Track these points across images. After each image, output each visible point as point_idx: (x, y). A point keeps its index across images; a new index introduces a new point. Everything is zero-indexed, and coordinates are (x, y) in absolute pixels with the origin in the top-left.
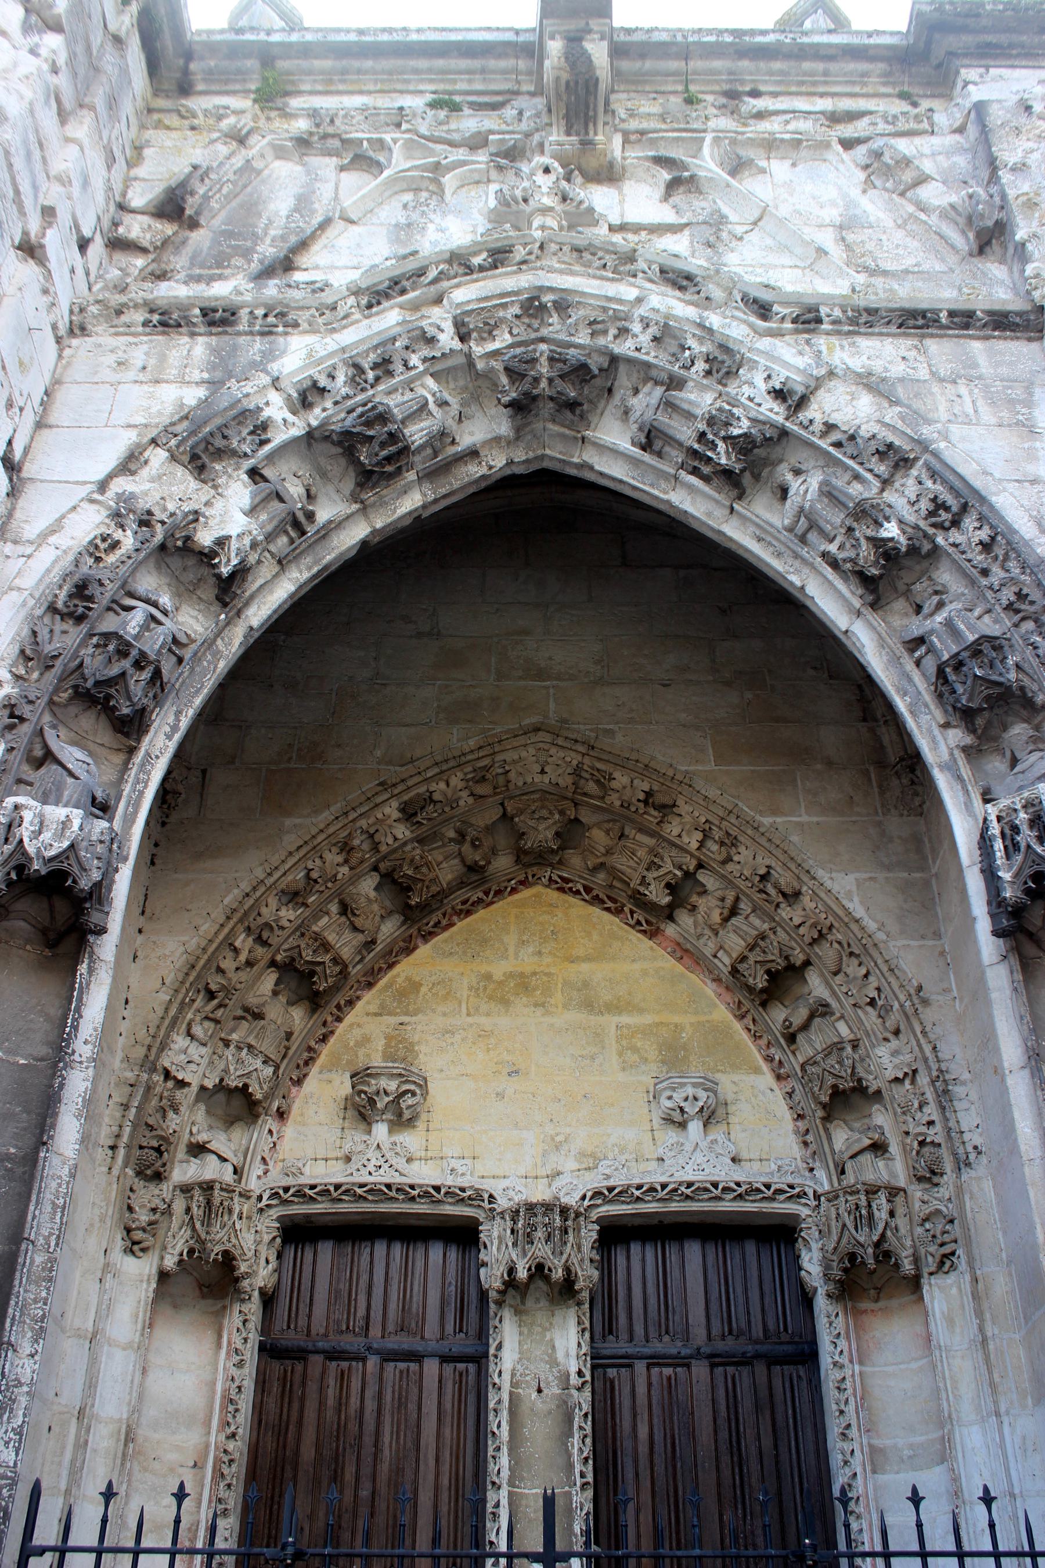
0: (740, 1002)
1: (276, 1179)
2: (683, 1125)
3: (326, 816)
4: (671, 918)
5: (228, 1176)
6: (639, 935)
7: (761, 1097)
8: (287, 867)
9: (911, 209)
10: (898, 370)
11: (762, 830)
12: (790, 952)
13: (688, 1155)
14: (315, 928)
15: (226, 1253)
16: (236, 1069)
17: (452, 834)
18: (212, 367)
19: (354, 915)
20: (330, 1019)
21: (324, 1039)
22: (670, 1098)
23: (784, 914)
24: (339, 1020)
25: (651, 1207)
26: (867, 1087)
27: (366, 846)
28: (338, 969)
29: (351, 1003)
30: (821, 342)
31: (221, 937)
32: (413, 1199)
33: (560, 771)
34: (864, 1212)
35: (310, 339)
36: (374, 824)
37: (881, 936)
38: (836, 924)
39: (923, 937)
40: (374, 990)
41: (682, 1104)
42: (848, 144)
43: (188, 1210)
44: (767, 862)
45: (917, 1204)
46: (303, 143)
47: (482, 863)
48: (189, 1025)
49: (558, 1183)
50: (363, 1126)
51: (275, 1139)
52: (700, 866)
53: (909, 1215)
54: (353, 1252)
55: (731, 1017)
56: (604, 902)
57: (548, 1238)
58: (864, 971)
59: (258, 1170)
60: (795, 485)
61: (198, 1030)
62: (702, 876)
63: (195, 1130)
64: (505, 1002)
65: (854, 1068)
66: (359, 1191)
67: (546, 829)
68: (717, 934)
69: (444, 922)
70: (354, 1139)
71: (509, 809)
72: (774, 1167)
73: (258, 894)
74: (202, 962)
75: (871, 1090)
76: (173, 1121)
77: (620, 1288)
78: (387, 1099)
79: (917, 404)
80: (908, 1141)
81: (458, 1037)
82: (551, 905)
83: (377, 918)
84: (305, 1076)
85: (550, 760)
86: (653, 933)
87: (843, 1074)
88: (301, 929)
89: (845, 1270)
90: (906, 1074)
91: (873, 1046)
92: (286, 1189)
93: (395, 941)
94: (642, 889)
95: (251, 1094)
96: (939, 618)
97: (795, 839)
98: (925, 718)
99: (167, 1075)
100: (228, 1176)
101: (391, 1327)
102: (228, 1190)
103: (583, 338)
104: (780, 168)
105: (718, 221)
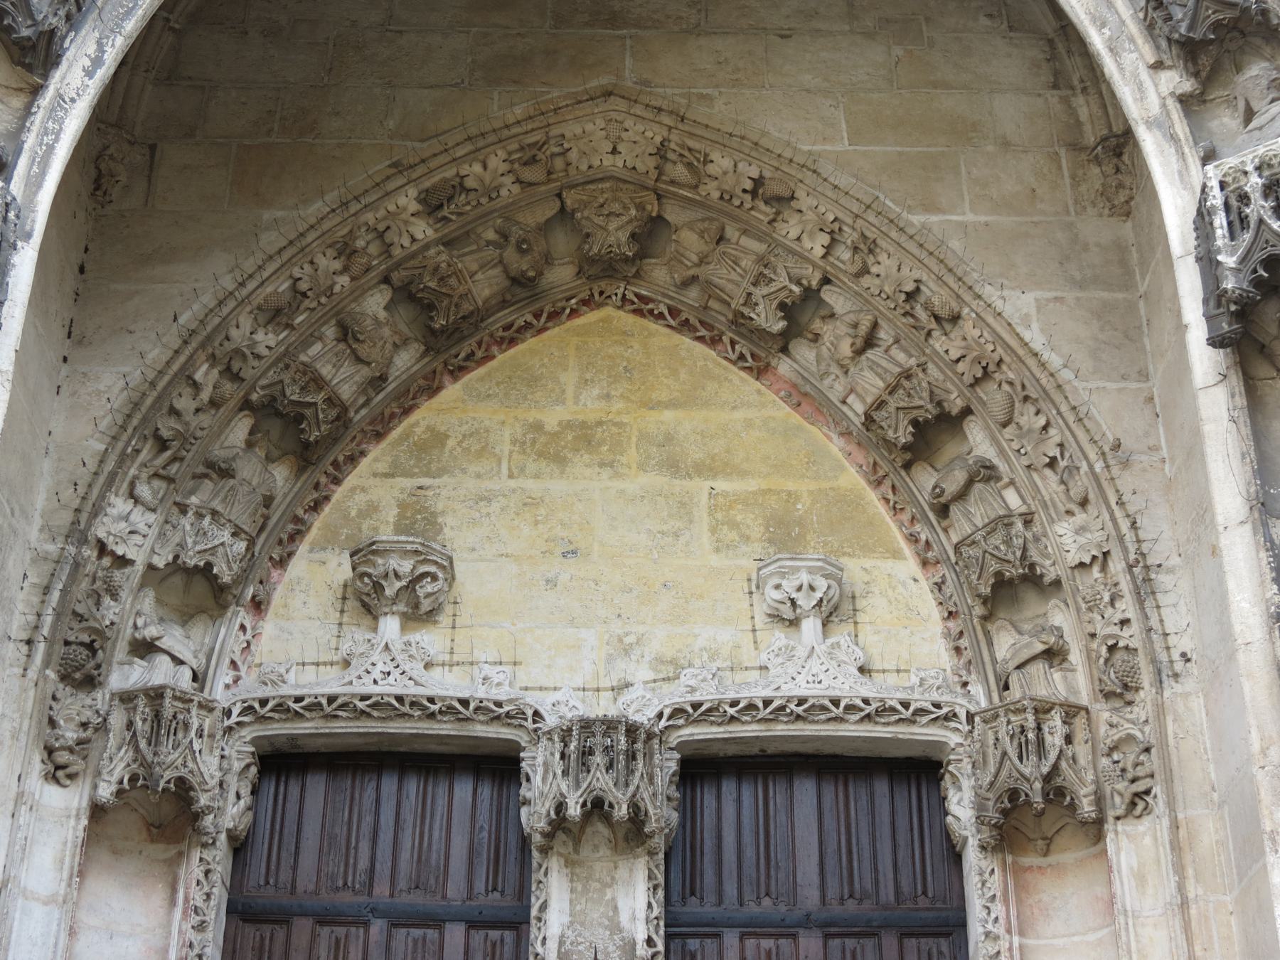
0: (875, 464)
1: (251, 688)
2: (794, 623)
3: (316, 208)
4: (785, 350)
5: (184, 680)
6: (743, 374)
7: (900, 589)
8: (265, 274)
11: (911, 231)
12: (944, 396)
13: (800, 662)
14: (303, 358)
15: (181, 781)
16: (195, 543)
17: (491, 235)
19: (358, 340)
20: (323, 480)
21: (316, 507)
22: (778, 587)
23: (937, 346)
24: (337, 481)
25: (750, 730)
26: (1042, 576)
27: (374, 249)
28: (334, 413)
29: (353, 460)
31: (175, 367)
32: (432, 716)
33: (638, 150)
34: (1031, 736)
36: (385, 219)
37: (1066, 375)
38: (1007, 359)
39: (1124, 378)
40: (384, 444)
41: (794, 595)
43: (130, 725)
44: (917, 274)
45: (1103, 729)
47: (531, 274)
48: (132, 485)
49: (627, 696)
50: (367, 620)
51: (249, 636)
52: (826, 281)
53: (1093, 741)
54: (353, 787)
55: (862, 483)
56: (696, 330)
57: (610, 767)
58: (1042, 421)
59: (226, 676)
61: (144, 491)
62: (828, 295)
63: (140, 622)
64: (560, 460)
65: (1025, 550)
66: (361, 705)
67: (617, 229)
68: (846, 373)
69: (480, 354)
70: (355, 638)
71: (569, 202)
72: (915, 680)
73: (225, 310)
74: (149, 401)
75: (1047, 580)
76: (110, 611)
77: (706, 835)
78: (398, 585)
80: (1094, 646)
81: (495, 506)
82: (625, 333)
83: (389, 346)
84: (290, 555)
85: (624, 135)
86: (760, 371)
87: (1010, 557)
88: (285, 358)
89: (1005, 813)
90: (1094, 558)
91: (1052, 521)
92: (263, 702)
93: (412, 378)
94: (746, 311)
95: (216, 577)
97: (955, 244)
98: (1129, 58)
99: (102, 549)
100: (184, 680)
101: (402, 884)
102: (184, 699)
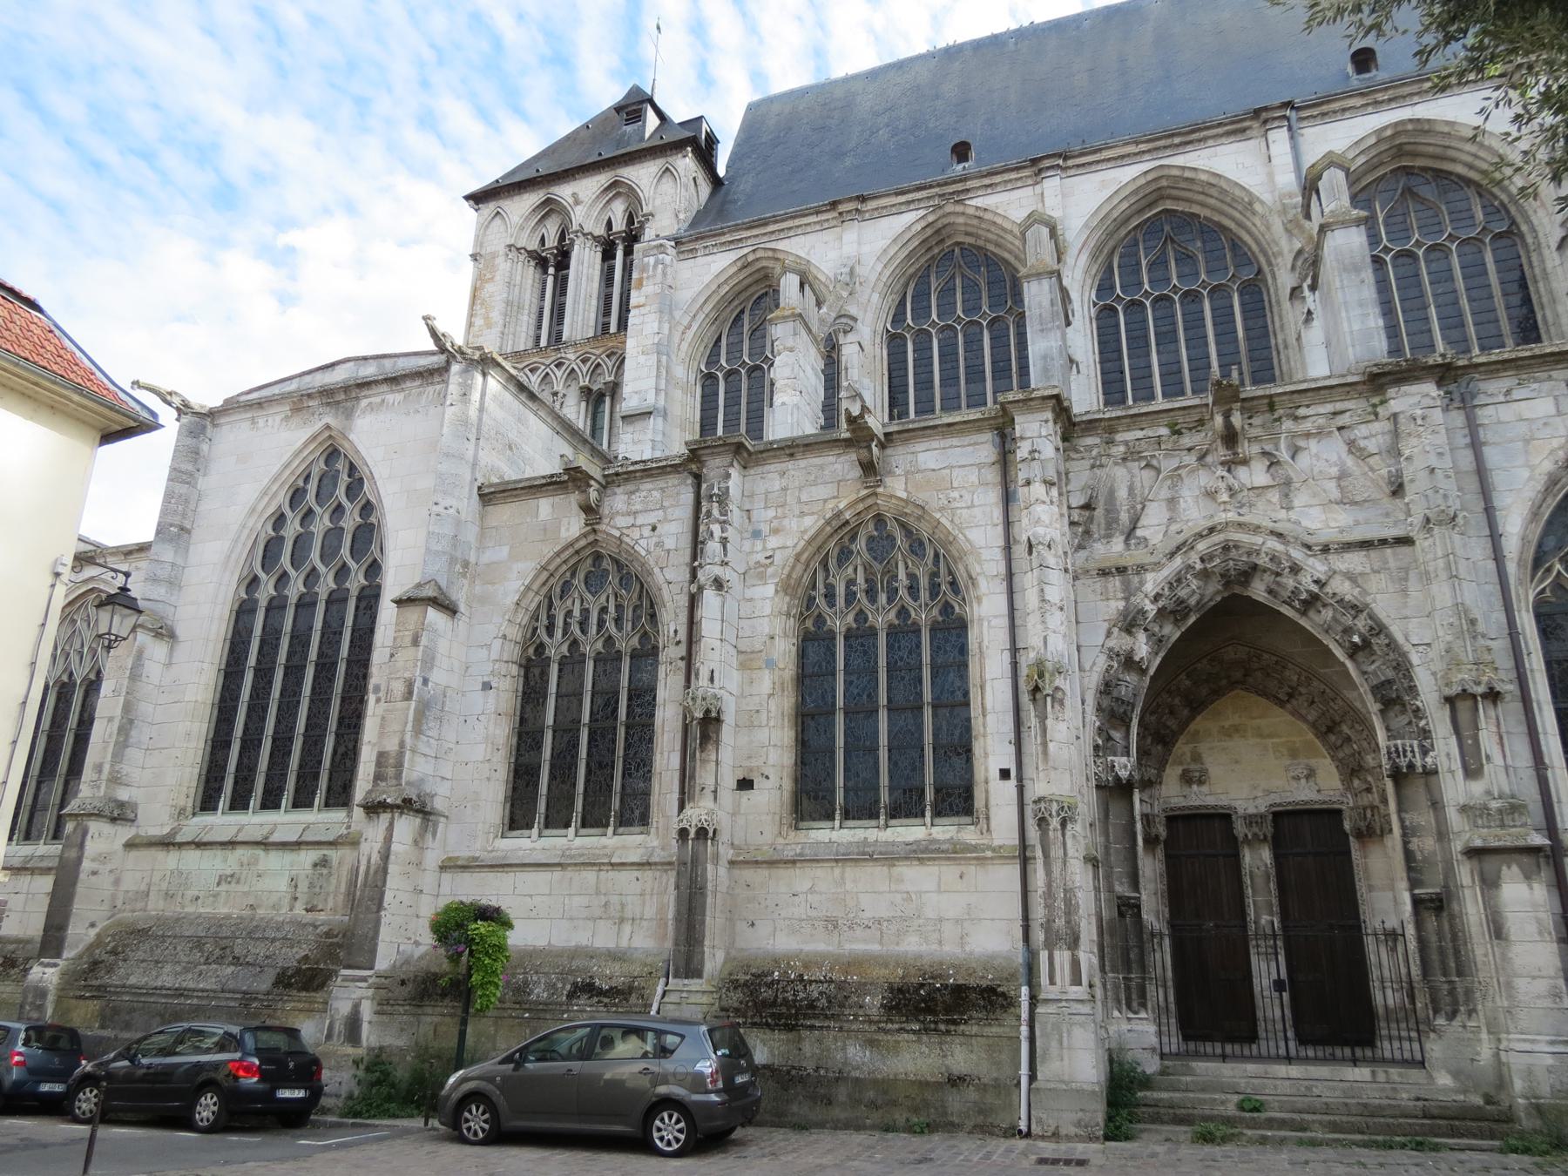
9: (1367, 469)
10: (1359, 569)
18: (1124, 591)
25: (1290, 808)
30: (1330, 557)
35: (1153, 574)
42: (1340, 429)
46: (1124, 459)
60: (1324, 612)
64: (1230, 736)
70: (1186, 790)
79: (1365, 586)
96: (1373, 667)
103: (1244, 559)
104: (1313, 445)
105: (1288, 483)
